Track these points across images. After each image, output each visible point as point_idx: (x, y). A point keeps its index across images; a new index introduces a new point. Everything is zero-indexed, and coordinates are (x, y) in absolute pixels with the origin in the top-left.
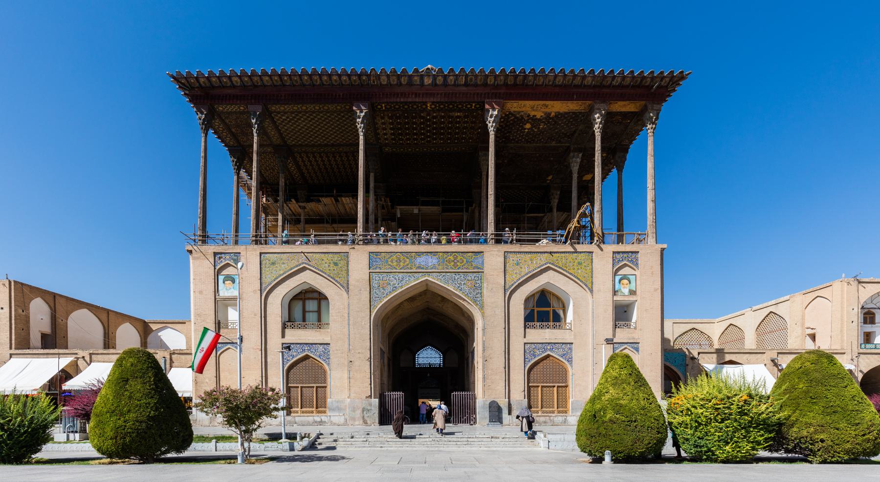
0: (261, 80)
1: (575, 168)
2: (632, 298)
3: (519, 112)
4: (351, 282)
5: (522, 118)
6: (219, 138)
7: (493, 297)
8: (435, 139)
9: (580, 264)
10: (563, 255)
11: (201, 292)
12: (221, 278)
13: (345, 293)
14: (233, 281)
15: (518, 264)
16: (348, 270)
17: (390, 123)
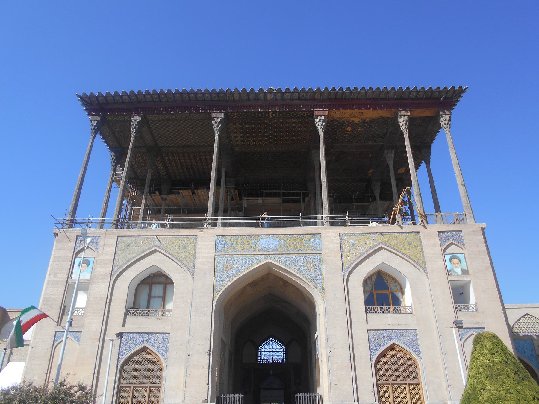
0: (145, 97)
1: (391, 162)
2: (466, 278)
3: (341, 118)
4: (197, 265)
5: (344, 123)
6: (105, 142)
7: (332, 279)
8: (276, 141)
9: (410, 244)
10: (393, 235)
11: (55, 275)
12: (77, 261)
13: (190, 277)
14: (88, 264)
15: (353, 245)
16: (195, 254)
17: (240, 128)
